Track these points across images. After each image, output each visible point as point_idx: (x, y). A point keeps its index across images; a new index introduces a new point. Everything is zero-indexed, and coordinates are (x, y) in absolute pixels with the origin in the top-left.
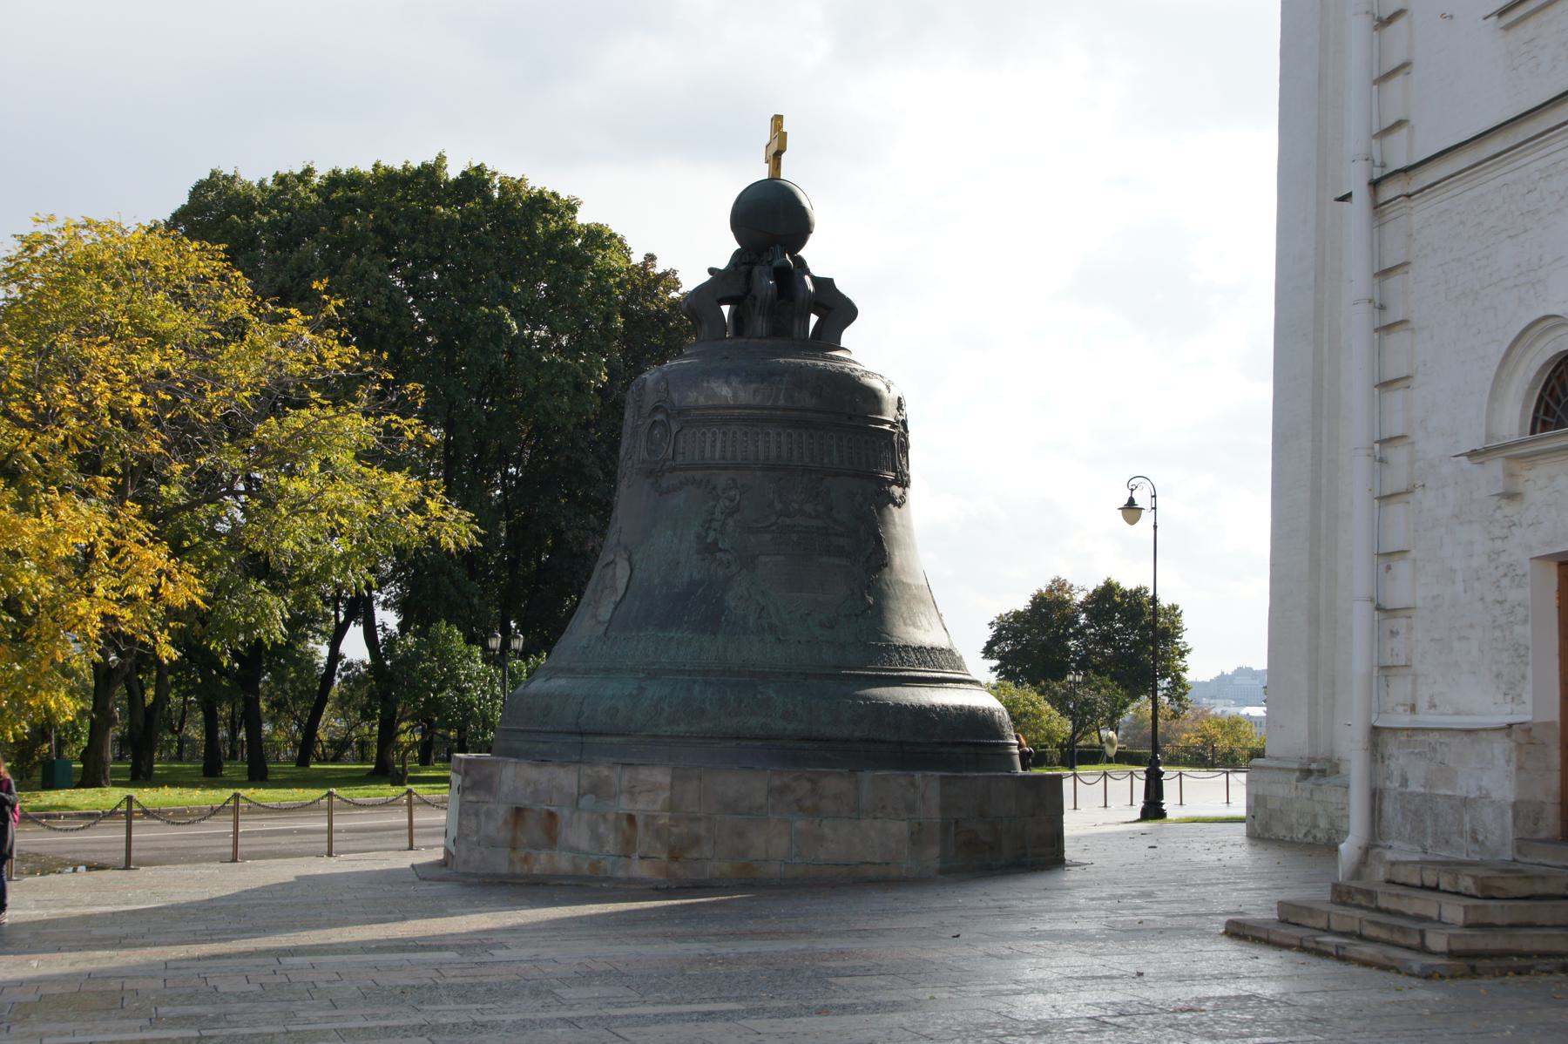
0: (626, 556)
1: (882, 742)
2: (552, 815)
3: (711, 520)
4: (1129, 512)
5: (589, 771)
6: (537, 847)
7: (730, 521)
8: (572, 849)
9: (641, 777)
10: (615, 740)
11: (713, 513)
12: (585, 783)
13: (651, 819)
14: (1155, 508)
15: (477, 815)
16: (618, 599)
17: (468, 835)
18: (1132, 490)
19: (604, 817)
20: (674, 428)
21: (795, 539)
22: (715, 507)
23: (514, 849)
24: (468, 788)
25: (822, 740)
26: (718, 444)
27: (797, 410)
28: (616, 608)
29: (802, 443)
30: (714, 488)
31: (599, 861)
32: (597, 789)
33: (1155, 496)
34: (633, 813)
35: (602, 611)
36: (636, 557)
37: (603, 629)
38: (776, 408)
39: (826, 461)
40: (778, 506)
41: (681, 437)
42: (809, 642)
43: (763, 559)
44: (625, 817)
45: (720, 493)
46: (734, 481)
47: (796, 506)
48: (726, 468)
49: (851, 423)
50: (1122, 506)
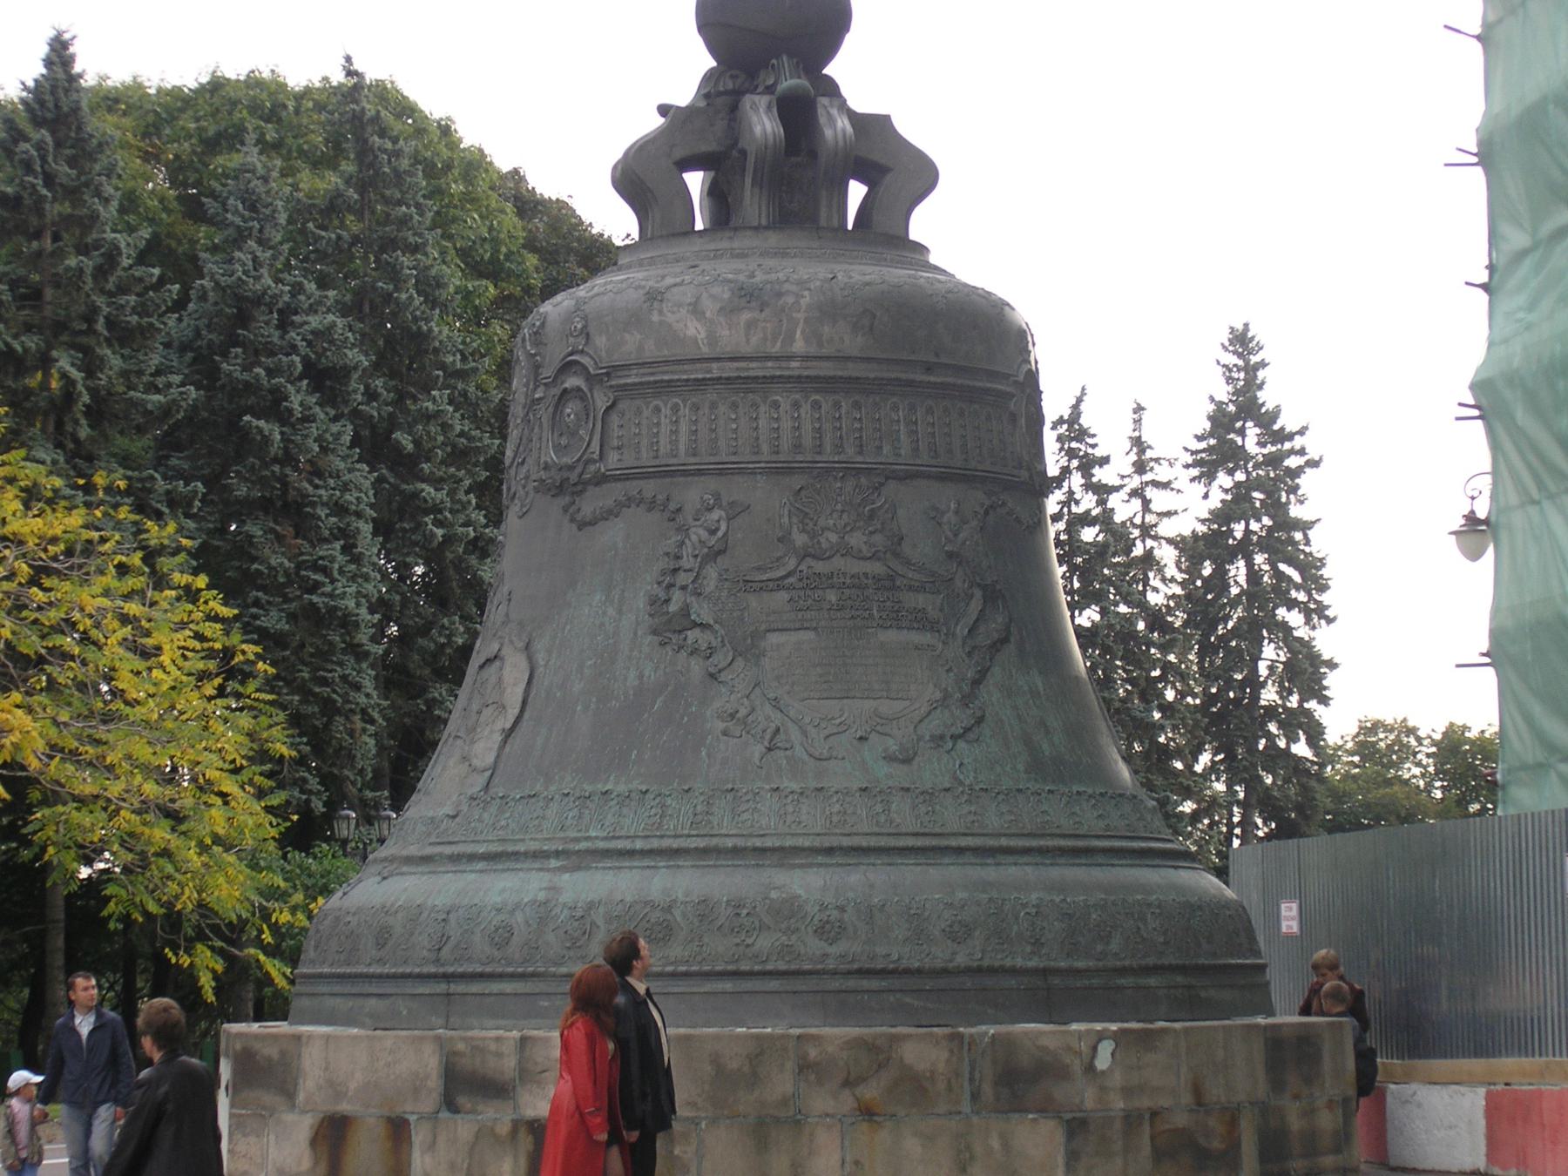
0: (521, 645)
1: (1013, 971)
3: (675, 570)
7: (712, 572)
10: (508, 987)
11: (678, 557)
16: (508, 725)
20: (601, 401)
21: (834, 599)
25: (893, 972)
26: (684, 427)
28: (505, 741)
35: (479, 747)
36: (540, 646)
37: (481, 780)
38: (790, 358)
39: (886, 449)
40: (800, 539)
41: (615, 419)
42: (865, 790)
43: (774, 638)
45: (690, 520)
46: (717, 496)
47: (833, 538)
48: (700, 472)
49: (932, 379)
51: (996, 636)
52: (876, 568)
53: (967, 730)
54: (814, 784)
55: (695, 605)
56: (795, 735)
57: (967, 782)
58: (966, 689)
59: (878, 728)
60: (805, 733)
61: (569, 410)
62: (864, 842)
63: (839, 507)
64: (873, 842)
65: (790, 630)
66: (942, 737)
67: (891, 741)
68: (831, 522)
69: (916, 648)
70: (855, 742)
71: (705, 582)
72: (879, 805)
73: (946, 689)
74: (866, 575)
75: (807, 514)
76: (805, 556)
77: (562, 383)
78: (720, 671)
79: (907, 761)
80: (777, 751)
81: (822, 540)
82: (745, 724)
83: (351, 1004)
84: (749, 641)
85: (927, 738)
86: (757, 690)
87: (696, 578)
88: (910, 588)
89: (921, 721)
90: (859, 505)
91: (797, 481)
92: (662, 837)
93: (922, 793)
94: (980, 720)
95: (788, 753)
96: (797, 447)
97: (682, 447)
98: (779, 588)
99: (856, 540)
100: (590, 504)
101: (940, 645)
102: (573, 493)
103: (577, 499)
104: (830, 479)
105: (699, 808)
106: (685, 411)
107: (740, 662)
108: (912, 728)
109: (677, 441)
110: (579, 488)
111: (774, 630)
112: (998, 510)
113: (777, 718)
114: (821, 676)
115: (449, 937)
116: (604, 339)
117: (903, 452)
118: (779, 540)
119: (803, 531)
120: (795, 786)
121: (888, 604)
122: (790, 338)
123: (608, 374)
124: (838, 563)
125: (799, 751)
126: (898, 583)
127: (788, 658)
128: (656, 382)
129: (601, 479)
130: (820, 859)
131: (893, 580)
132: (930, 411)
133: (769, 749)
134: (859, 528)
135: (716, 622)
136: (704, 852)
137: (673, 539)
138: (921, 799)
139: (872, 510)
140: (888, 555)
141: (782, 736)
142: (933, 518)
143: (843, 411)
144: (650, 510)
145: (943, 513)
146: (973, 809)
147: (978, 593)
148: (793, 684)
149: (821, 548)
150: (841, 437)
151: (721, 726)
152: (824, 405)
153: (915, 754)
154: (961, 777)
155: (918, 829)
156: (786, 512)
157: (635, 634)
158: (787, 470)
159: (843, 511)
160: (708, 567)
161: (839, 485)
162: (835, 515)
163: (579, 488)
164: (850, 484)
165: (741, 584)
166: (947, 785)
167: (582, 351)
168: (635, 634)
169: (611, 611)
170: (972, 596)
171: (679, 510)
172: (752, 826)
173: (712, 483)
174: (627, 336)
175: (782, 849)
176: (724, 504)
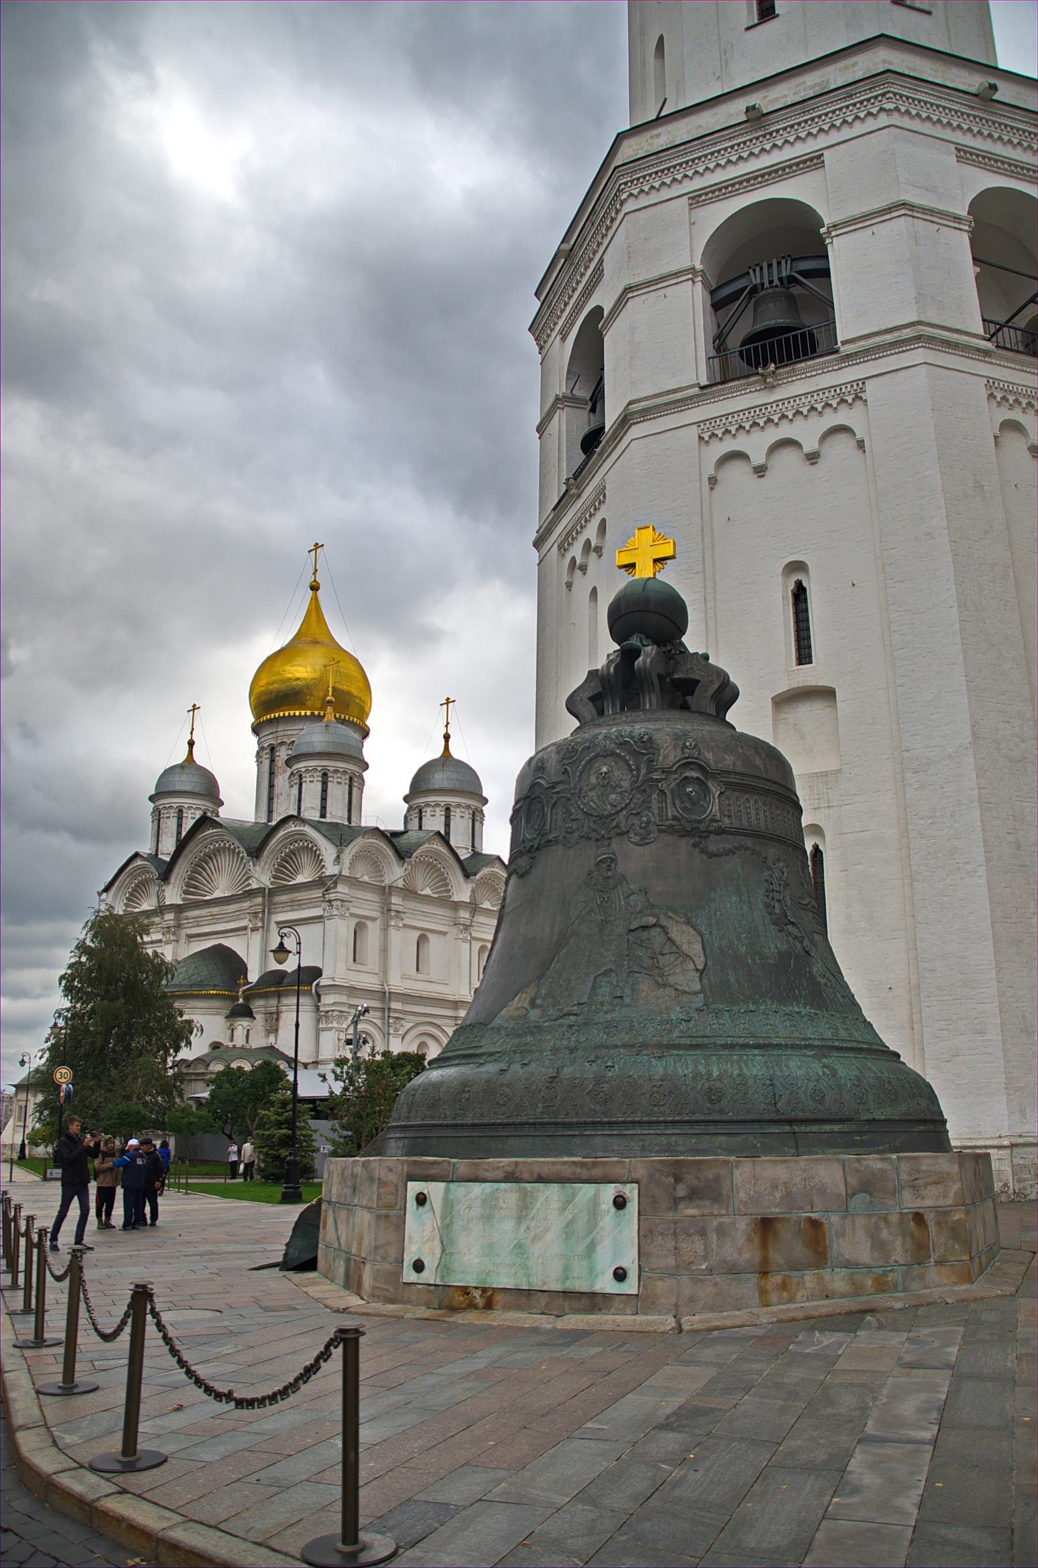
2: (815, 1224)
4: (281, 956)
5: (856, 1165)
6: (796, 1266)
8: (848, 1264)
9: (924, 1168)
10: (836, 1128)
12: (853, 1181)
13: (942, 1213)
14: (299, 953)
15: (703, 1233)
17: (692, 1262)
18: (282, 937)
19: (886, 1220)
23: (764, 1273)
24: (682, 1198)
31: (885, 1274)
32: (868, 1186)
33: (299, 943)
34: (921, 1211)
44: (910, 1216)
61: (690, 789)
77: (682, 773)
83: (694, 1140)
100: (713, 844)
102: (700, 837)
103: (703, 841)
110: (705, 835)
115: (781, 1096)
116: (711, 754)
123: (719, 774)
129: (721, 832)
163: (705, 835)
167: (697, 758)
174: (726, 756)
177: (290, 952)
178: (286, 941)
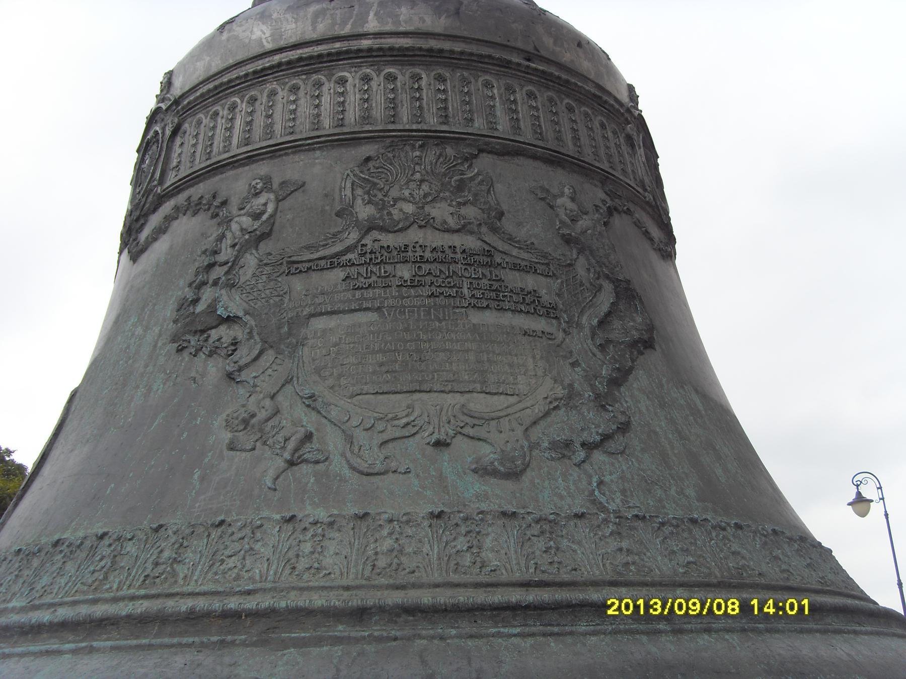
3: (211, 266)
7: (251, 260)
14: (883, 499)
18: (858, 486)
21: (407, 275)
22: (222, 237)
27: (405, 34)
29: (419, 89)
30: (224, 203)
33: (880, 488)
40: (364, 211)
42: (440, 515)
43: (319, 324)
45: (235, 211)
47: (409, 208)
48: (251, 159)
50: (851, 500)
51: (636, 335)
52: (470, 242)
53: (606, 438)
54: (353, 510)
55: (225, 298)
56: (334, 441)
57: (612, 507)
58: (602, 388)
59: (468, 430)
60: (350, 440)
62: (426, 598)
63: (418, 176)
64: (444, 597)
65: (343, 312)
66: (568, 444)
67: (485, 449)
68: (406, 193)
69: (525, 333)
70: (430, 450)
71: (241, 272)
72: (461, 539)
73: (571, 386)
74: (453, 248)
75: (375, 184)
76: (369, 230)
78: (240, 369)
79: (514, 475)
80: (304, 467)
81: (395, 212)
82: (261, 430)
84: (286, 329)
85: (546, 444)
86: (289, 388)
87: (231, 268)
88: (516, 267)
89: (535, 423)
90: (445, 175)
91: (367, 150)
92: (95, 601)
93: (538, 521)
94: (624, 428)
95: (321, 467)
96: (366, 118)
97: (235, 141)
98: (332, 267)
99: (441, 211)
101: (561, 335)
104: (408, 148)
105: (166, 554)
106: (243, 106)
107: (270, 355)
108: (519, 431)
109: (230, 137)
111: (321, 314)
112: (624, 215)
113: (309, 421)
114: (381, 365)
117: (500, 127)
118: (339, 214)
119: (370, 202)
120: (322, 514)
121: (485, 282)
122: (363, 19)
124: (414, 235)
125: (338, 465)
126: (498, 260)
127: (335, 345)
128: (216, 88)
130: (341, 629)
131: (491, 256)
132: (530, 95)
133: (291, 463)
134: (445, 199)
135: (247, 313)
136: (141, 622)
137: (215, 235)
138: (536, 529)
139: (461, 180)
140: (484, 229)
141: (315, 445)
142: (543, 199)
143: (424, 83)
144: (195, 214)
145: (555, 197)
146: (624, 544)
147: (608, 287)
148: (340, 376)
149: (392, 219)
150: (421, 108)
151: (227, 436)
152: (400, 77)
153: (527, 466)
154: (603, 500)
155: (530, 574)
156: (349, 185)
157: (155, 346)
158: (353, 140)
159: (422, 181)
160: (248, 255)
161: (418, 153)
162: (413, 185)
164: (431, 155)
165: (284, 268)
166: (579, 510)
168: (155, 346)
169: (139, 331)
170: (600, 288)
171: (224, 203)
172: (238, 578)
173: (263, 168)
175: (271, 612)
176: (275, 186)
177: (872, 501)
178: (862, 489)
